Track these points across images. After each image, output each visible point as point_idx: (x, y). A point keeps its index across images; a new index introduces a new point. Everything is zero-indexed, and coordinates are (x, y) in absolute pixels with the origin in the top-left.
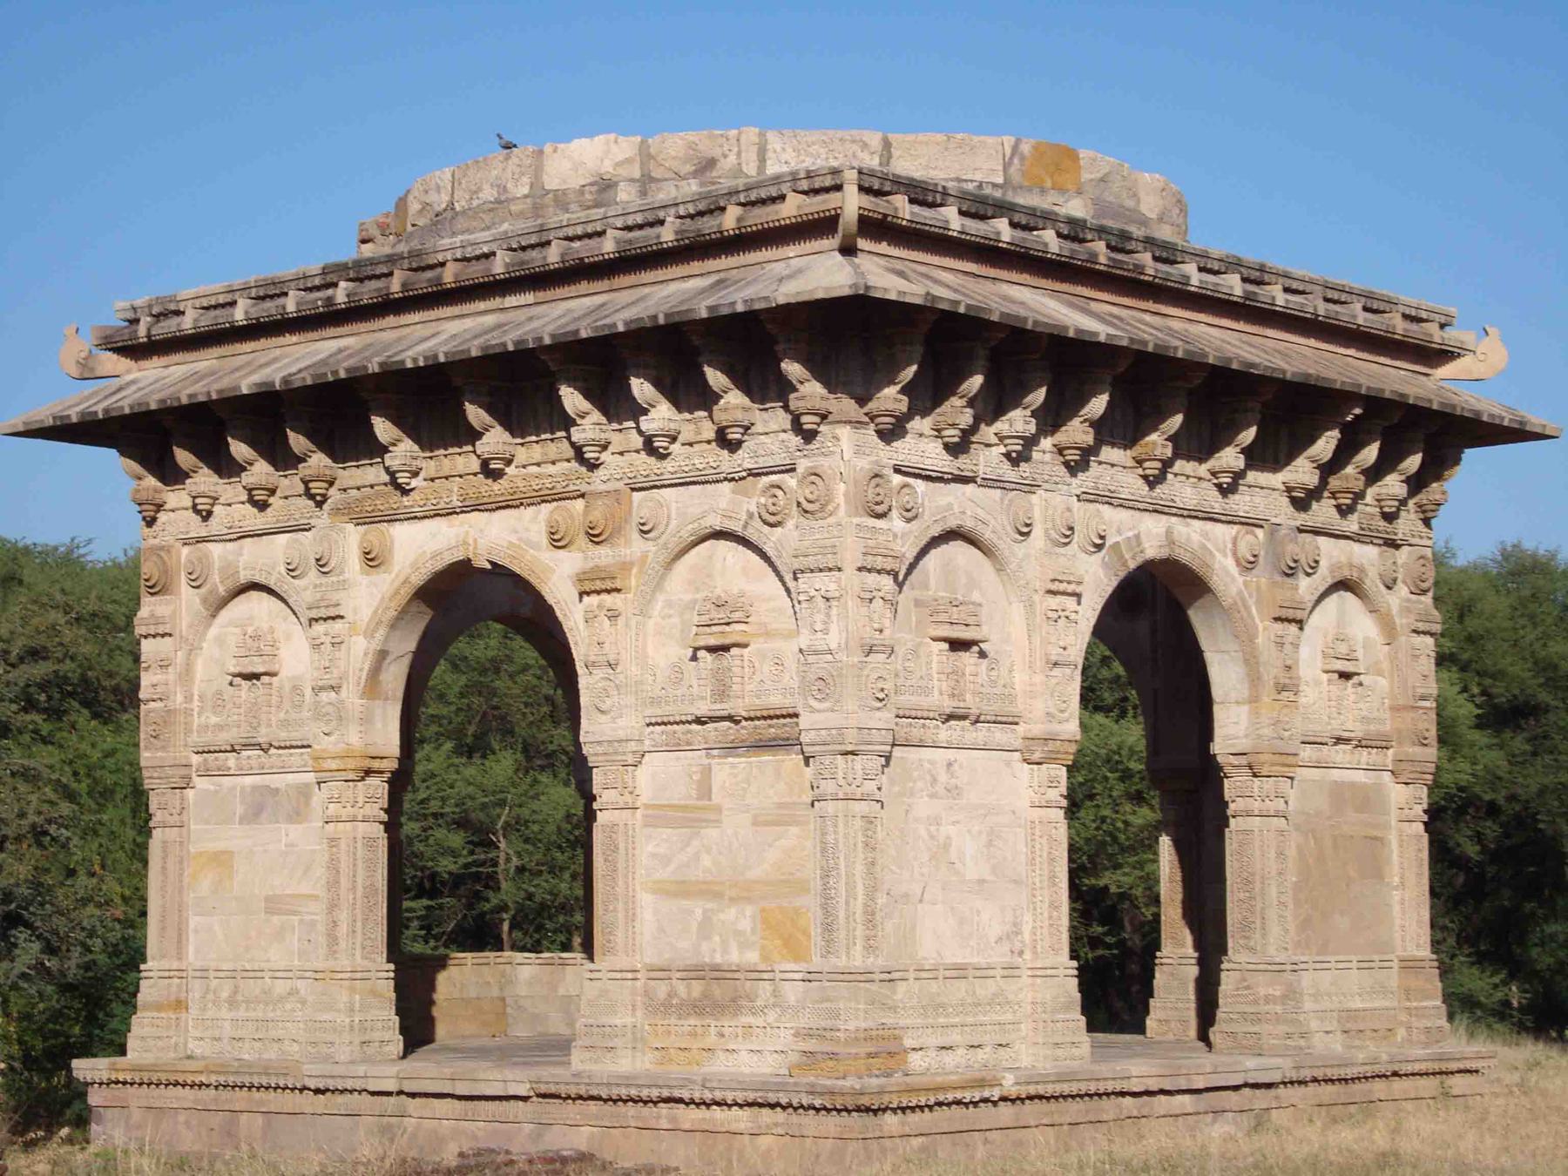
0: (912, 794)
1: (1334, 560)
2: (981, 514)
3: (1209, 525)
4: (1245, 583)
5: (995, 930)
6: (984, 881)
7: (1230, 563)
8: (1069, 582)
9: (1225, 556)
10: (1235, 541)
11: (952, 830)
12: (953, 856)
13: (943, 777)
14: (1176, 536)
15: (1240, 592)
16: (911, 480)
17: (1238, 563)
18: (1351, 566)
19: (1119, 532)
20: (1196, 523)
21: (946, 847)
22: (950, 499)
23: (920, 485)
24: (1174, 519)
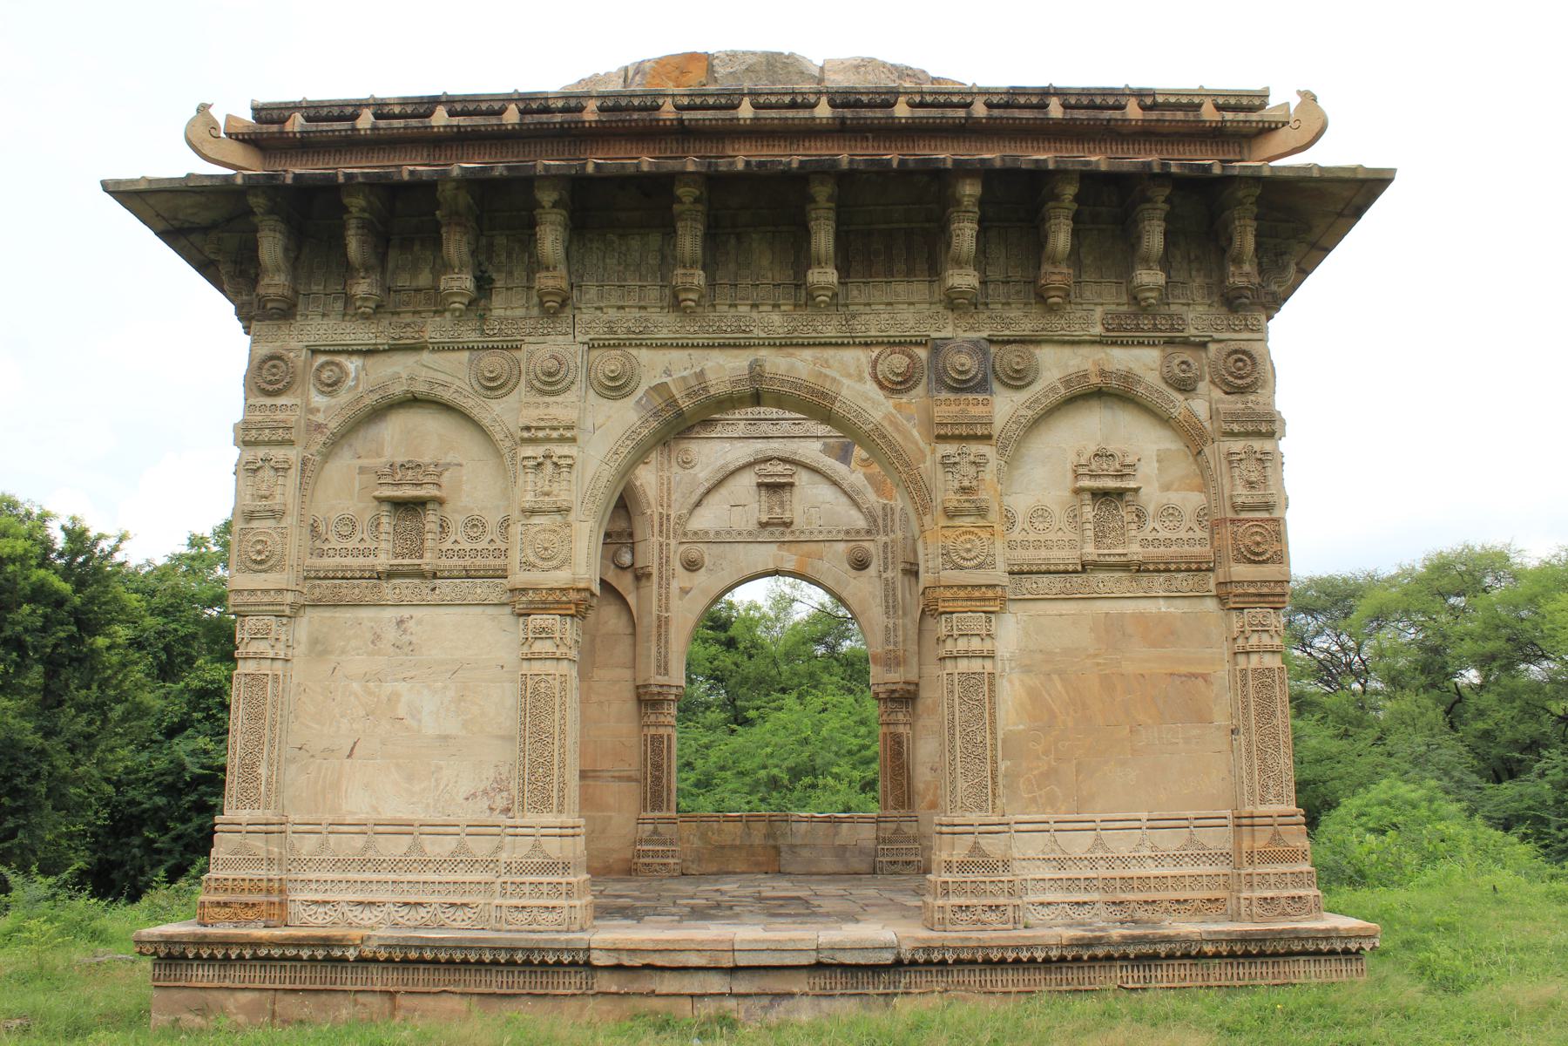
0: (343, 652)
1: (1071, 370)
2: (441, 377)
3: (829, 353)
4: (898, 407)
5: (465, 788)
6: (445, 738)
7: (871, 388)
8: (554, 429)
9: (861, 379)
10: (875, 364)
11: (402, 687)
12: (401, 711)
13: (391, 634)
14: (769, 368)
15: (887, 416)
16: (338, 359)
17: (881, 386)
18: (1103, 373)
19: (667, 372)
20: (808, 354)
21: (393, 698)
22: (396, 369)
23: (352, 365)
24: (763, 353)
